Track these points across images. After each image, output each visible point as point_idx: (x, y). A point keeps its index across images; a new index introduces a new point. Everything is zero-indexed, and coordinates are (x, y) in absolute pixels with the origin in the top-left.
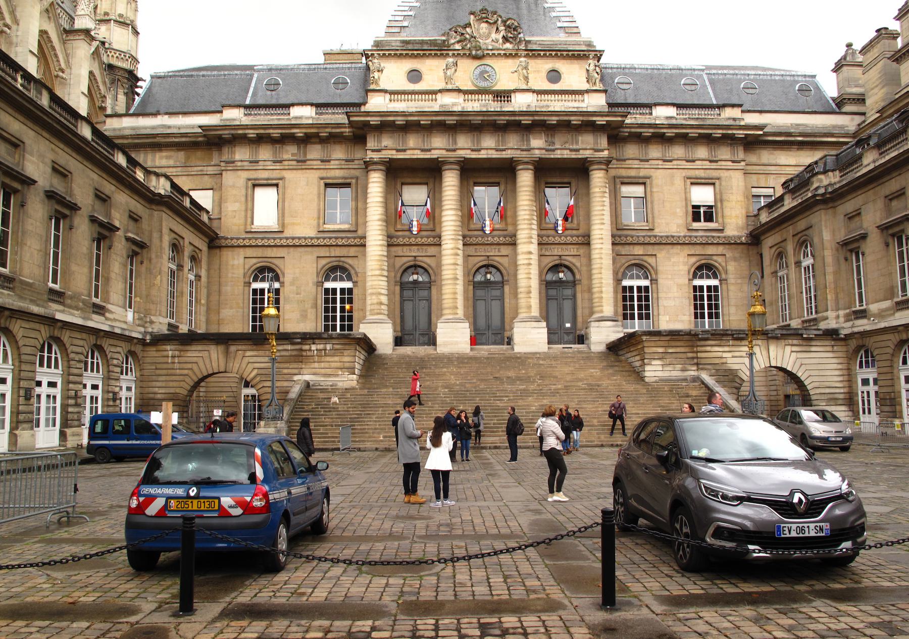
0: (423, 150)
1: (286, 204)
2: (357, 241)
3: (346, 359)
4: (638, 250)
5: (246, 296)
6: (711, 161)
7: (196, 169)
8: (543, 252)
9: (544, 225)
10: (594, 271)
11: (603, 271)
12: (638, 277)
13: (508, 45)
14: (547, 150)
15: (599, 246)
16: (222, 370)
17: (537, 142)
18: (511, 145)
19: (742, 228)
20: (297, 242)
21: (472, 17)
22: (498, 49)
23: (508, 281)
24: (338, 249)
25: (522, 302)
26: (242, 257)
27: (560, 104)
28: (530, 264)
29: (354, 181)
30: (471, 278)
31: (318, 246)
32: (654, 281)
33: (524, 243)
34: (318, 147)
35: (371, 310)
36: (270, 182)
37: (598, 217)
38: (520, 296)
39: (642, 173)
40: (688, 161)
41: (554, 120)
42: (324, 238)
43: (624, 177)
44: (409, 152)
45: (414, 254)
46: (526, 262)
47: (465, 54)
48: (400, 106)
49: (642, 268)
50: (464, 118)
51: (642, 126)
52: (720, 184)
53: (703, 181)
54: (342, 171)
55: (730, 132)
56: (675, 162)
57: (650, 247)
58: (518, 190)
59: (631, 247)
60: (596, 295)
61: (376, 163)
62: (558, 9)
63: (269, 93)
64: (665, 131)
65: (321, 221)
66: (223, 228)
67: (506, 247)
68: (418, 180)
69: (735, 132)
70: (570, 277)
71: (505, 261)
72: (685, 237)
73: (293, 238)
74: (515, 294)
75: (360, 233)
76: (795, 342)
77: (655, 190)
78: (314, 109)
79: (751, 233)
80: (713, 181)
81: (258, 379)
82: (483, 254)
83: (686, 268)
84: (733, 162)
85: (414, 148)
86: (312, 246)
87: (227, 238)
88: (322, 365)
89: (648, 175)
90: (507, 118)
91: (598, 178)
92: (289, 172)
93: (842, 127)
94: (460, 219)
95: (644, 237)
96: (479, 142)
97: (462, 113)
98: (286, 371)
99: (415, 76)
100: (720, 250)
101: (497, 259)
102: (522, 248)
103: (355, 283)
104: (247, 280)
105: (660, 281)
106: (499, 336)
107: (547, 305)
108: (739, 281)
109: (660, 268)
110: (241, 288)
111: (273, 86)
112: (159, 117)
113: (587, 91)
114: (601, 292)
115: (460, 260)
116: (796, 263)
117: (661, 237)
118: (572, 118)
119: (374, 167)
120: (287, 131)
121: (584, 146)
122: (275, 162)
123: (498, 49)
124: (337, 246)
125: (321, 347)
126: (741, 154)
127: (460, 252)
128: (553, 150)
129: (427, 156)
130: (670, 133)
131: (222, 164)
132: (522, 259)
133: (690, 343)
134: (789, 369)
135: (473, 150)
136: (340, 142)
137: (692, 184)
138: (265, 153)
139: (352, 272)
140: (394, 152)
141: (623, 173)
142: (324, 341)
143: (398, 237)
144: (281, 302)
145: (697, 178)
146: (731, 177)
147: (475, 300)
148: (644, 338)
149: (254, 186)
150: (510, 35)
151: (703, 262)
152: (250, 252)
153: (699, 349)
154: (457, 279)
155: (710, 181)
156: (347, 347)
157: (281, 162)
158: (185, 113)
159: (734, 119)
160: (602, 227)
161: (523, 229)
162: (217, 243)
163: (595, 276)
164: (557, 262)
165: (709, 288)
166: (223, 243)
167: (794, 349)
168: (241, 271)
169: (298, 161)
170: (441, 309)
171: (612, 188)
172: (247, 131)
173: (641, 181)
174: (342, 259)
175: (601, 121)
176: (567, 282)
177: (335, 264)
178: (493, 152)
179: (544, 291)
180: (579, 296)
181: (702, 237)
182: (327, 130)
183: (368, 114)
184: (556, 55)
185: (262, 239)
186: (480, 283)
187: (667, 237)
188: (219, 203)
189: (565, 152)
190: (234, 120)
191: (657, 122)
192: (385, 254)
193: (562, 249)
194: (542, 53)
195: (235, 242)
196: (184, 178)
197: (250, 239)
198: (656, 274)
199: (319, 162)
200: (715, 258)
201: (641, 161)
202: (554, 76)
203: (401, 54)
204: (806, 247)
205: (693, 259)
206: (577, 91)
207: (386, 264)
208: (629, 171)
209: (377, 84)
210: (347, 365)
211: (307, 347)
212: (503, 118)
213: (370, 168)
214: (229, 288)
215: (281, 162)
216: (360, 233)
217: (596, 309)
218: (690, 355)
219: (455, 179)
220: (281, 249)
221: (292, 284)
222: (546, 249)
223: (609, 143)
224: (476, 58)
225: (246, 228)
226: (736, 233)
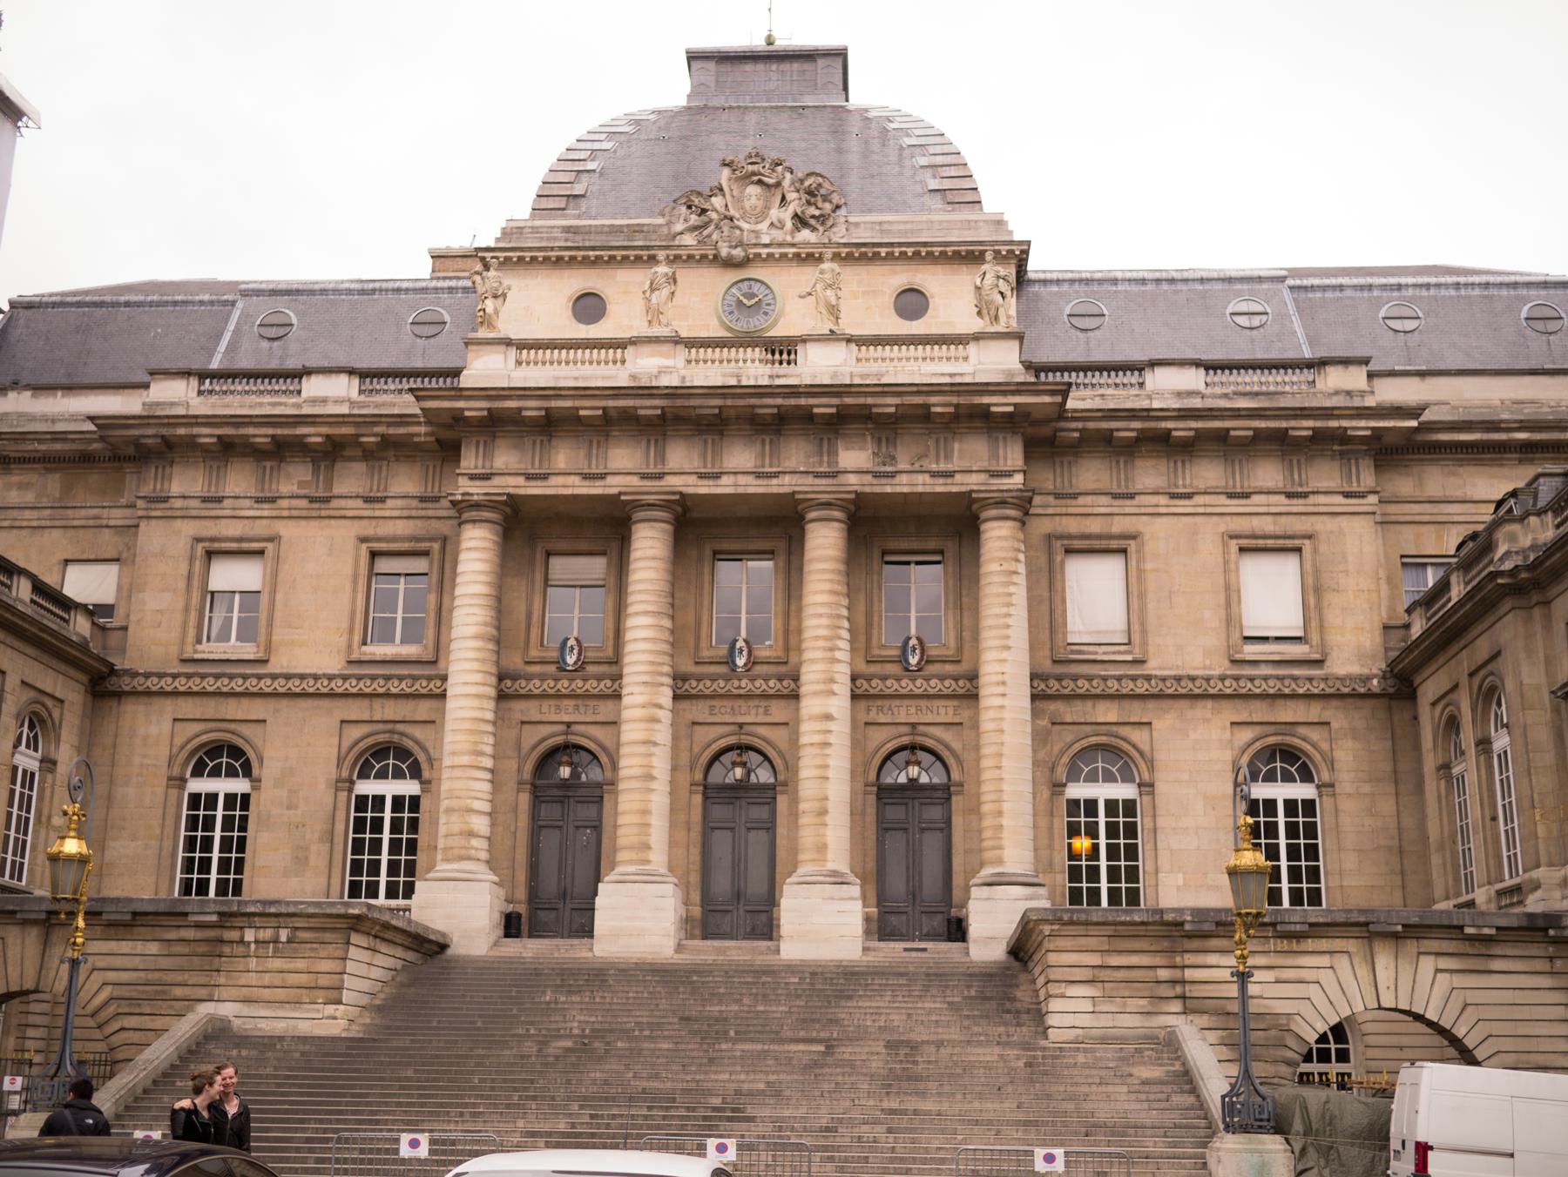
1: (279, 596)
2: (434, 686)
3: (325, 966)
4: (1107, 713)
5: (171, 811)
6: (1290, 495)
7: (83, 513)
8: (873, 716)
9: (876, 652)
10: (985, 763)
11: (1005, 762)
12: (1109, 778)
13: (805, 235)
14: (876, 475)
15: (997, 701)
16: (29, 985)
17: (854, 460)
18: (791, 464)
19: (1373, 657)
21: (726, 172)
22: (780, 245)
23: (785, 784)
24: (390, 703)
25: (807, 836)
26: (168, 718)
28: (827, 744)
29: (436, 546)
30: (699, 776)
31: (346, 695)
32: (1147, 787)
33: (815, 693)
34: (360, 467)
35: (445, 849)
36: (245, 546)
37: (994, 633)
38: (803, 820)
39: (1118, 525)
40: (1231, 496)
41: (889, 404)
42: (359, 678)
43: (1070, 537)
44: (554, 481)
45: (566, 718)
46: (817, 738)
47: (704, 257)
49: (1112, 755)
50: (679, 402)
51: (1113, 414)
52: (1315, 550)
53: (1270, 543)
54: (411, 523)
55: (1333, 424)
56: (1199, 499)
57: (1136, 704)
58: (806, 568)
59: (1089, 703)
60: (987, 822)
61: (477, 506)
62: (932, 150)
63: (265, 344)
64: (1170, 425)
65: (357, 638)
66: (131, 652)
67: (782, 703)
68: (583, 546)
69: (1345, 423)
70: (938, 779)
71: (778, 736)
72: (1222, 678)
73: (288, 677)
74: (794, 814)
76: (1445, 946)
77: (1149, 566)
78: (356, 381)
79: (1392, 665)
80: (1297, 542)
81: (111, 1010)
82: (728, 719)
83: (1228, 755)
84: (1347, 495)
85: (566, 474)
86: (332, 695)
87: (135, 674)
88: (267, 979)
90: (779, 401)
91: (998, 537)
92: (291, 523)
94: (666, 636)
95: (1119, 679)
98: (178, 992)
99: (589, 306)
100: (1314, 712)
101: (761, 730)
102: (810, 705)
103: (426, 784)
104: (176, 772)
105: (1161, 788)
106: (764, 917)
107: (880, 843)
108: (1366, 788)
109: (1160, 756)
110: (160, 790)
111: (276, 331)
112: (12, 395)
113: (977, 337)
114: (1000, 813)
115: (663, 734)
116: (1477, 745)
117: (1164, 679)
119: (474, 514)
120: (286, 431)
121: (965, 465)
122: (259, 500)
123: (780, 245)
124: (387, 695)
125: (266, 934)
126: (1368, 478)
127: (665, 716)
128: (892, 475)
129: (596, 489)
130: (1182, 429)
131: (140, 503)
132: (809, 732)
133: (1166, 944)
134: (1431, 1015)
135: (701, 476)
136: (410, 458)
137: (1242, 550)
138: (239, 481)
139: (422, 758)
140: (521, 480)
141: (1072, 526)
142: (273, 922)
144: (251, 825)
145: (1255, 537)
146: (1341, 532)
147: (708, 828)
148: (1047, 929)
149: (210, 554)
151: (1272, 740)
152: (187, 708)
153: (1190, 959)
154: (650, 777)
155: (1289, 543)
156: (328, 936)
157: (273, 500)
158: (70, 388)
159: (1349, 393)
160: (1005, 655)
161: (813, 661)
162: (113, 683)
163: (986, 775)
164: (905, 740)
165: (1291, 806)
166: (126, 684)
167: (1445, 963)
168: (164, 752)
169: (312, 500)
170: (615, 851)
171: (1043, 560)
172: (196, 431)
173: (1114, 544)
174: (399, 727)
175: (1001, 405)
176: (931, 787)
177: (381, 738)
178: (750, 480)
179: (871, 811)
180: (957, 821)
181: (1266, 678)
182: (377, 429)
184: (917, 254)
185: (217, 677)
186: (723, 788)
187: (1178, 679)
188: (128, 590)
189: (920, 478)
190: (172, 404)
191: (1156, 405)
192: (490, 716)
193: (919, 709)
194: (883, 252)
196: (56, 533)
197: (189, 676)
198: (1151, 769)
199: (359, 503)
200: (1302, 730)
201: (1116, 496)
202: (912, 302)
203: (559, 259)
204: (1499, 704)
205: (1246, 735)
207: (491, 740)
209: (491, 326)
210: (324, 981)
211: (233, 935)
212: (769, 401)
213: (466, 516)
214: (131, 791)
215: (273, 500)
216: (441, 665)
217: (988, 855)
218: (1164, 974)
219: (657, 544)
220: (259, 702)
221: (279, 783)
222: (880, 709)
223: (1028, 457)
224: (729, 264)
225: (182, 651)
226: (1356, 669)
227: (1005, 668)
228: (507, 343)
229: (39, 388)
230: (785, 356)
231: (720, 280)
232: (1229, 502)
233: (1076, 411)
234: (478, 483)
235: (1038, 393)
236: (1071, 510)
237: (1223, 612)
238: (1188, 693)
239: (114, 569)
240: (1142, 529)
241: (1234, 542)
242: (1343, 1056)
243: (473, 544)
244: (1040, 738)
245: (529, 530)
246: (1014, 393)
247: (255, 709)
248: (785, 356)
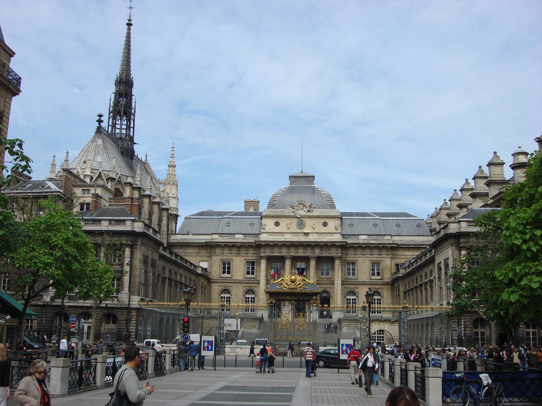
2: (257, 282)
4: (352, 286)
20: (237, 281)
32: (357, 297)
34: (244, 249)
39: (355, 259)
41: (322, 244)
48: (271, 238)
49: (353, 293)
75: (258, 279)
85: (276, 253)
91: (337, 262)
93: (429, 241)
96: (298, 250)
99: (277, 224)
100: (381, 286)
103: (256, 295)
113: (335, 233)
130: (364, 246)
138: (226, 251)
152: (221, 284)
158: (198, 234)
166: (212, 281)
168: (218, 291)
175: (338, 244)
183: (261, 241)
188: (211, 266)
195: (216, 281)
202: (325, 224)
206: (332, 234)
227: (338, 281)
228: (267, 233)
229: (193, 234)
231: (296, 220)
238: (364, 284)
239: (207, 263)
242: (383, 334)
244: (342, 290)
245: (270, 260)
247: (231, 285)
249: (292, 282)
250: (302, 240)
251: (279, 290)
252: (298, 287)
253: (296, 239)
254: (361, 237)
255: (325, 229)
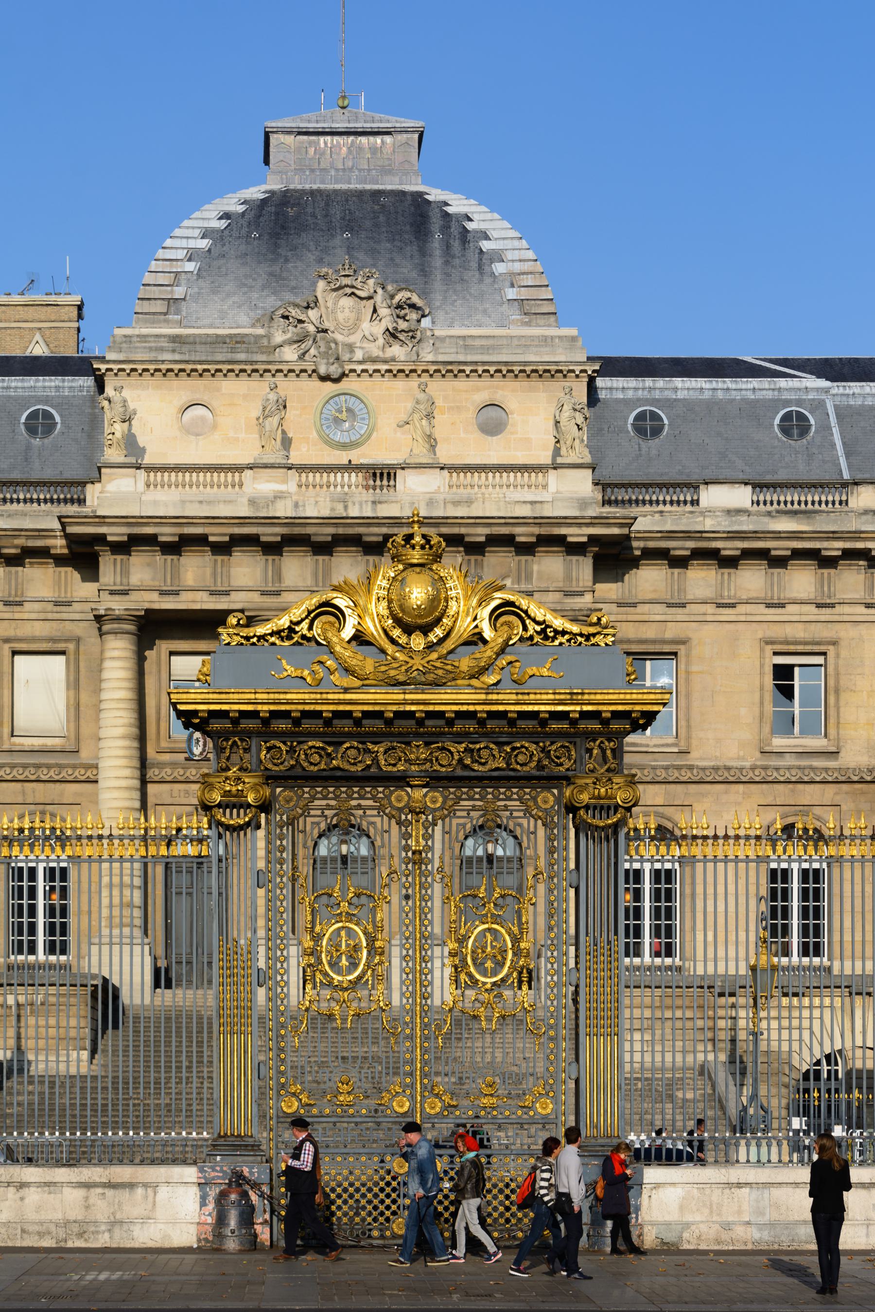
0: (213, 593)
2: (78, 774)
27: (497, 493)
39: (671, 632)
40: (769, 606)
41: (479, 534)
44: (184, 596)
50: (297, 530)
51: (670, 535)
53: (800, 648)
56: (741, 608)
61: (118, 619)
80: (822, 648)
89: (682, 636)
97: (292, 522)
100: (829, 793)
118: (517, 530)
121: (543, 585)
140: (155, 596)
143: (161, 765)
145: (787, 643)
150: (403, 325)
173: (667, 648)
175: (577, 535)
182: (17, 542)
183: (102, 520)
200: (817, 811)
201: (670, 605)
208: (643, 627)
213: (106, 628)
230: (385, 482)
232: (767, 611)
233: (639, 532)
234: (117, 598)
235: (609, 525)
236: (630, 618)
237: (757, 710)
240: (690, 636)
241: (769, 647)
243: (116, 654)
246: (588, 525)
248: (385, 482)
249: (408, 630)
250: (354, 512)
251: (297, 698)
252: (465, 664)
253: (315, 504)
254: (714, 497)
255: (494, 451)
